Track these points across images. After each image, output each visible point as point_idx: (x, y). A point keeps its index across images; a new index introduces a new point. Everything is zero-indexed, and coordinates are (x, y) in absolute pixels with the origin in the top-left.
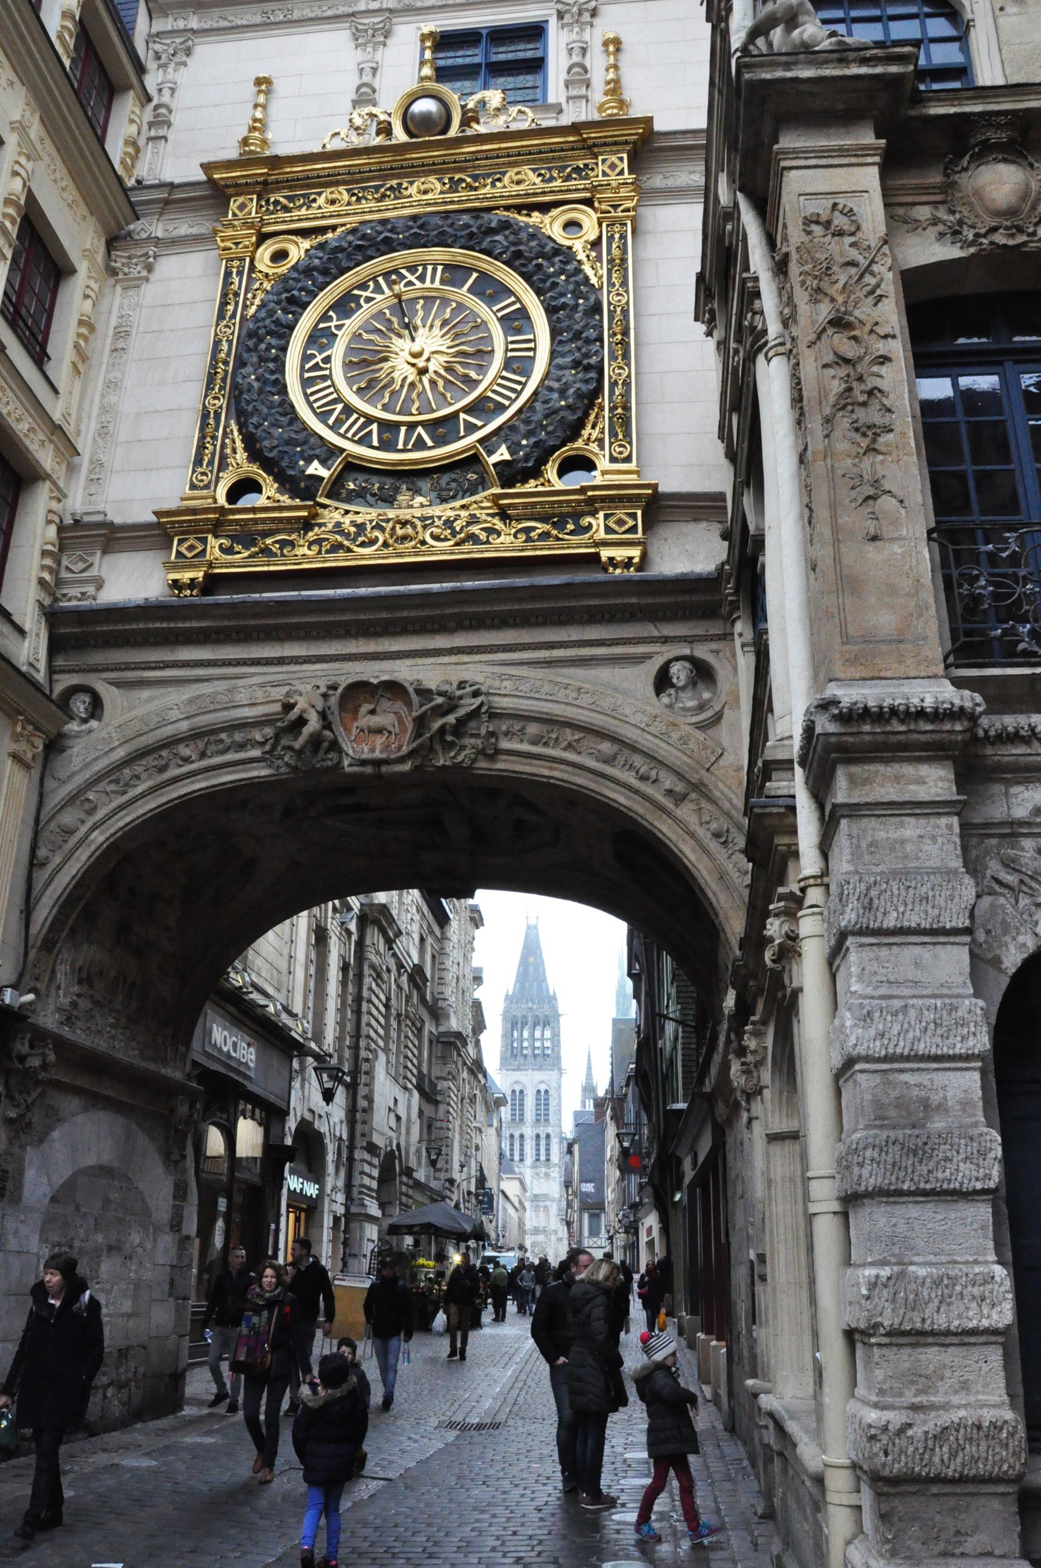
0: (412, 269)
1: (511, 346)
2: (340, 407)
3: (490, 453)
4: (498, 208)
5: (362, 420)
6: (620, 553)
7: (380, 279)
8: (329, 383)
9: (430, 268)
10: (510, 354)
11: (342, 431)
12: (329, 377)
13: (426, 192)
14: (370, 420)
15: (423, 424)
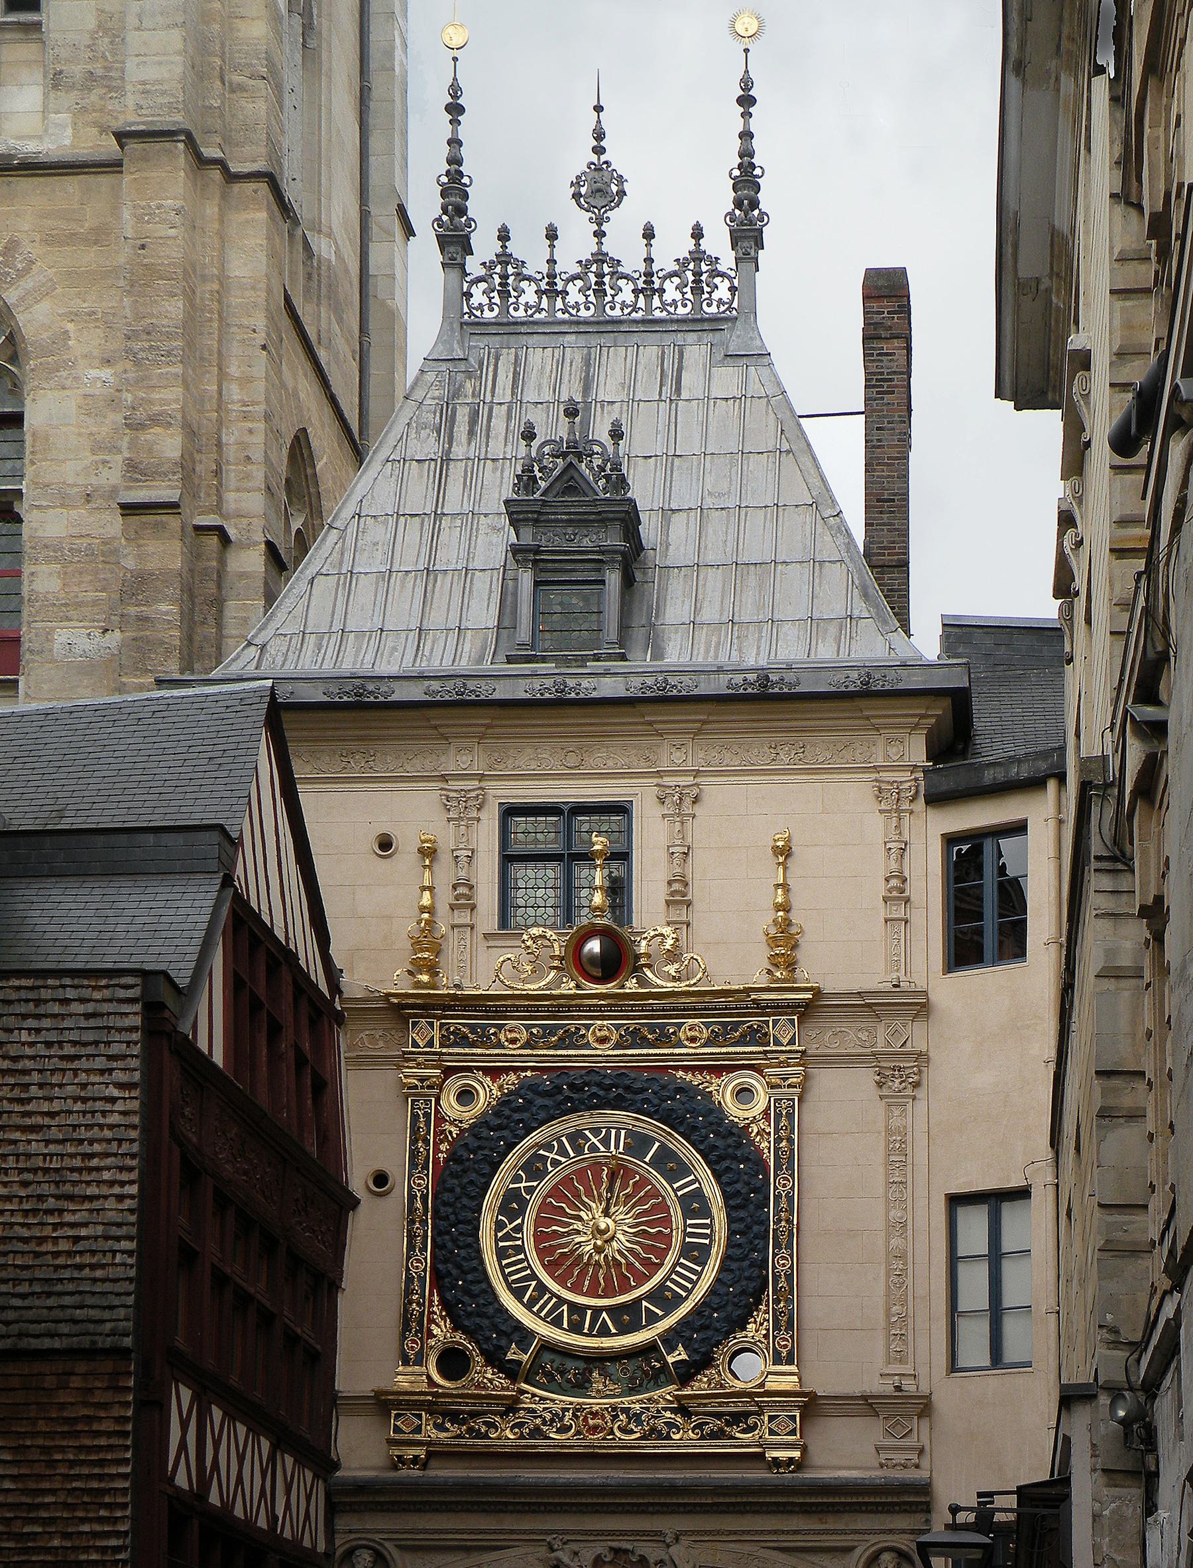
0: (596, 1131)
1: (689, 1230)
2: (534, 1283)
3: (671, 1349)
4: (676, 1068)
5: (554, 1300)
6: (782, 1454)
7: (564, 1139)
8: (522, 1256)
9: (613, 1131)
10: (688, 1240)
11: (535, 1309)
12: (520, 1249)
13: (603, 1040)
14: (561, 1301)
15: (609, 1310)
